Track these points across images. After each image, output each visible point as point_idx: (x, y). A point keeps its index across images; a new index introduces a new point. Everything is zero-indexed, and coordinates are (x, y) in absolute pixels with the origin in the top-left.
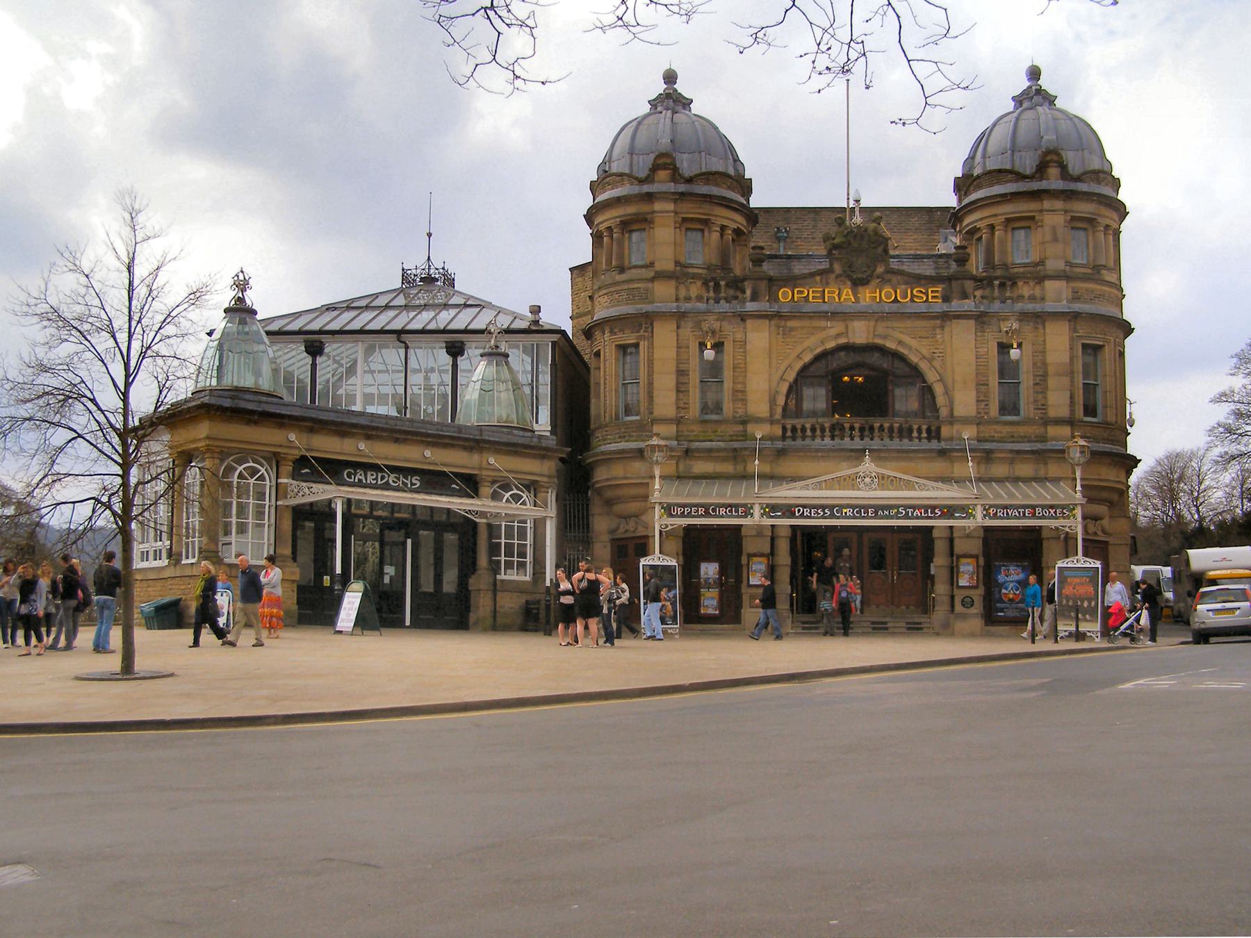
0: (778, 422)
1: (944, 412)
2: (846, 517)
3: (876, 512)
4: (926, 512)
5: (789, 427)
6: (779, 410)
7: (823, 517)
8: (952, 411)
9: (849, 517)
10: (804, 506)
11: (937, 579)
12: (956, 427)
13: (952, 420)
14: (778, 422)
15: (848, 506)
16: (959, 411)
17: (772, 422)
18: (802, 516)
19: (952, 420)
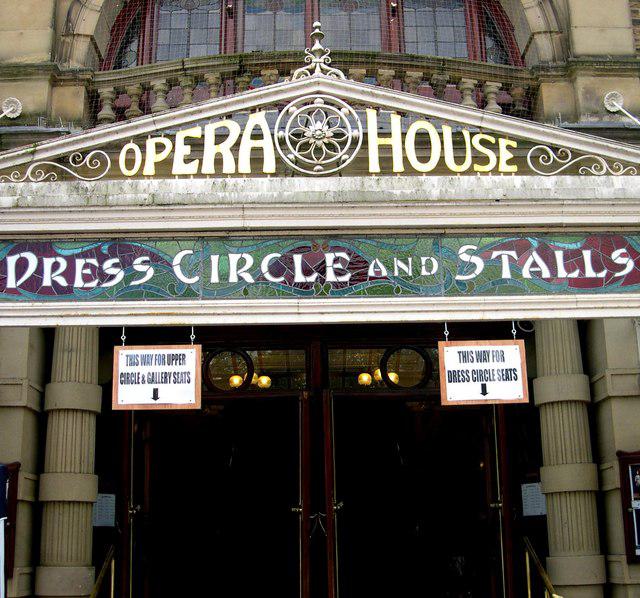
0: (74, 77)
1: (545, 48)
2: (225, 290)
3: (358, 267)
4: (574, 260)
5: (106, 92)
6: (80, 50)
7: (127, 293)
8: (567, 43)
9: (244, 291)
10: (44, 245)
11: (557, 533)
12: (583, 81)
13: (569, 64)
14: (74, 77)
15: (225, 238)
16: (586, 43)
17: (57, 78)
18: (34, 287)
19: (569, 64)
